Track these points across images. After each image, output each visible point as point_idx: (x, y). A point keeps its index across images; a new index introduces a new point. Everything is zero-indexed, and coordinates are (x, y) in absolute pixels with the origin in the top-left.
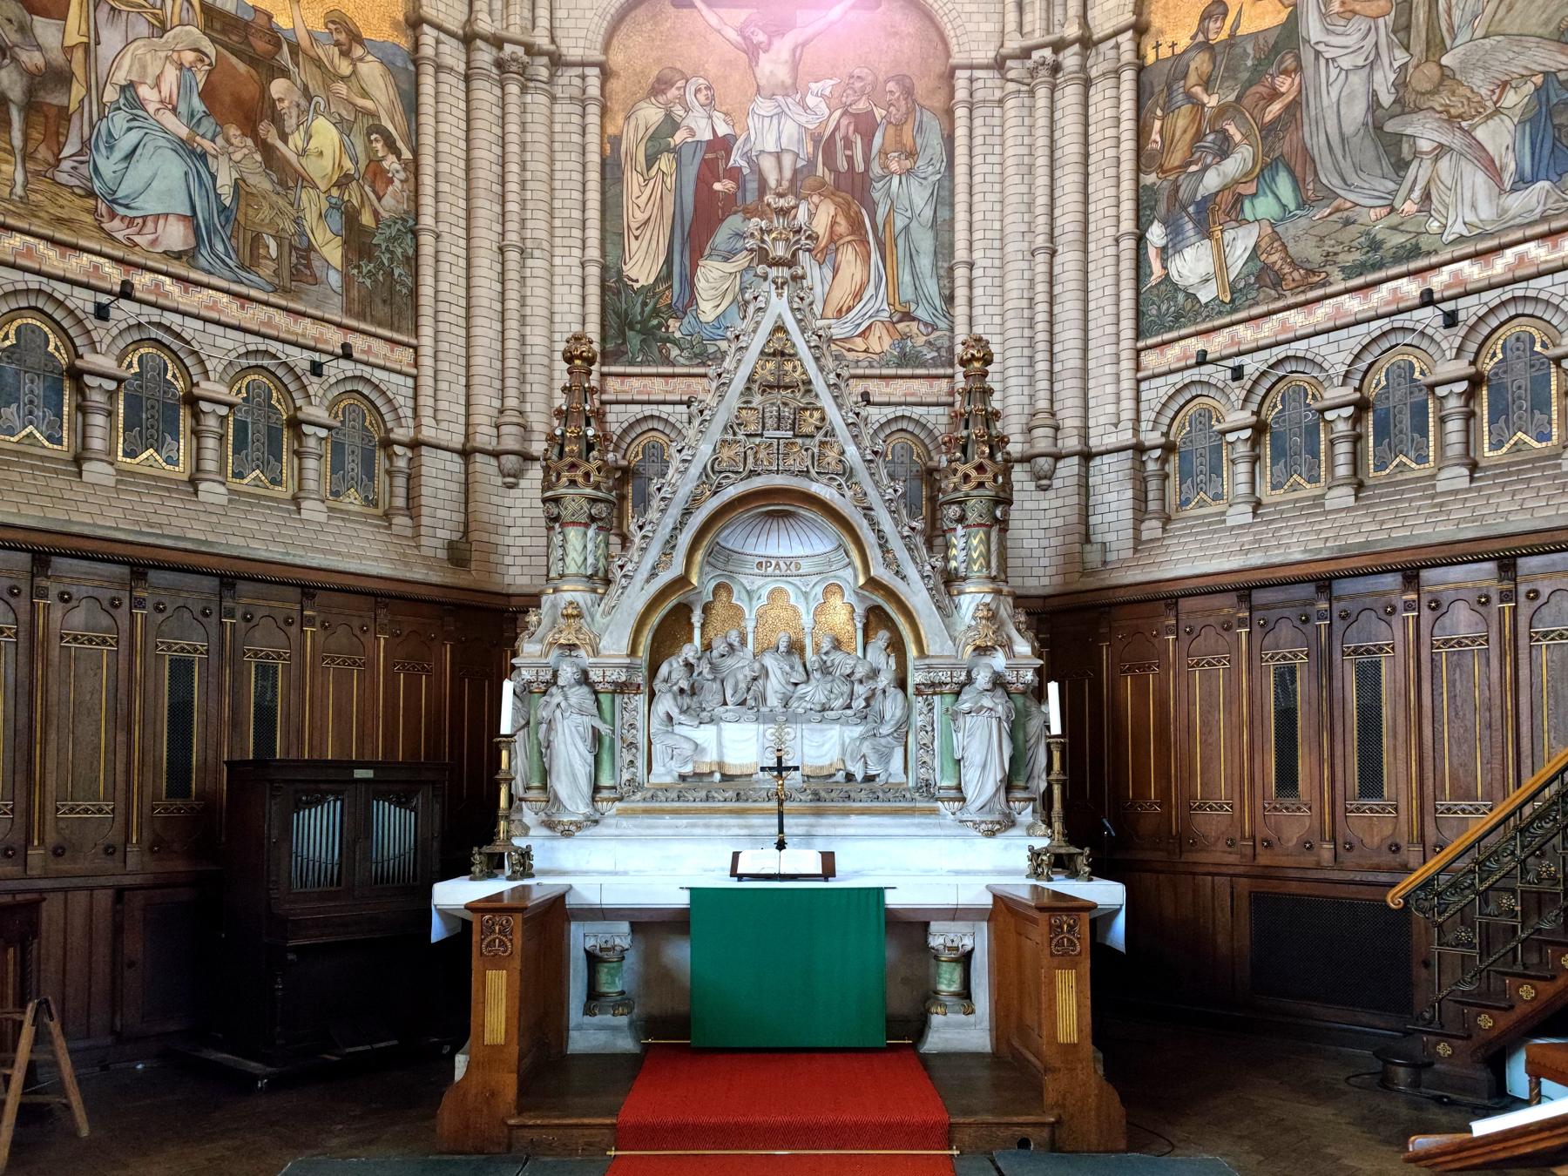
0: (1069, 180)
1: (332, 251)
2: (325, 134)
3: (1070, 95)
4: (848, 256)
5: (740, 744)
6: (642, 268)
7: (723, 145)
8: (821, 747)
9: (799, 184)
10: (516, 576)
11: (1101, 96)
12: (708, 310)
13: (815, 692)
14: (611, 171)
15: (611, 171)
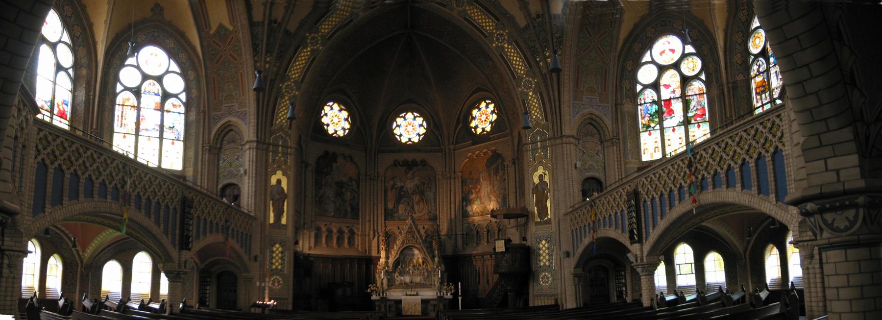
0: (453, 194)
1: (349, 210)
2: (349, 193)
3: (452, 181)
4: (421, 204)
5: (407, 279)
6: (390, 206)
7: (402, 187)
8: (418, 279)
9: (414, 193)
10: (374, 254)
11: (457, 181)
12: (400, 212)
13: (416, 272)
14: (386, 192)
15: (386, 192)
